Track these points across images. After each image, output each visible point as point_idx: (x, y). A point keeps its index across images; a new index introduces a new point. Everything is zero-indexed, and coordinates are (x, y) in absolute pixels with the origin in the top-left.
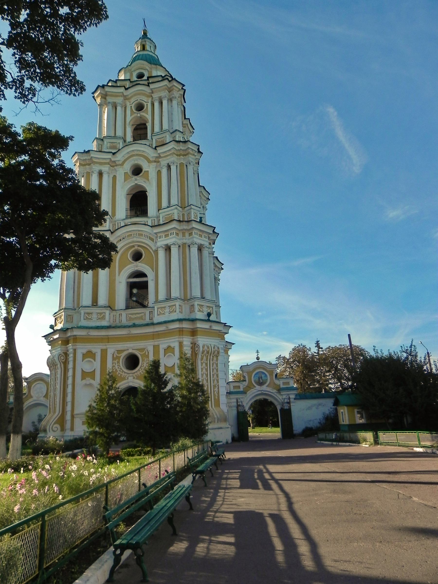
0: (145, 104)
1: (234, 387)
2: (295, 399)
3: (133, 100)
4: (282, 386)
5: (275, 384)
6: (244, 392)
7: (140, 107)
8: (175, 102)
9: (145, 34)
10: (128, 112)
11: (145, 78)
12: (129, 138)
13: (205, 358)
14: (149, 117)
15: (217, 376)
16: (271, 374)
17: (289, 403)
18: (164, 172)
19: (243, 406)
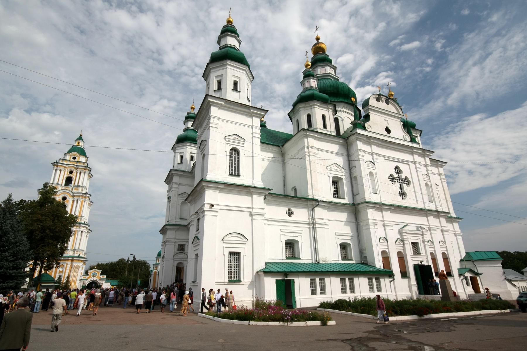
0: (74, 172)
1: (84, 277)
2: (105, 282)
3: (69, 169)
4: (101, 278)
5: (99, 277)
6: (87, 280)
7: (71, 172)
8: (86, 175)
9: (81, 135)
10: (66, 173)
11: (76, 160)
12: (63, 184)
13: (74, 269)
14: (74, 177)
15: (77, 274)
16: (98, 274)
17: (102, 283)
18: (75, 202)
19: (85, 284)
